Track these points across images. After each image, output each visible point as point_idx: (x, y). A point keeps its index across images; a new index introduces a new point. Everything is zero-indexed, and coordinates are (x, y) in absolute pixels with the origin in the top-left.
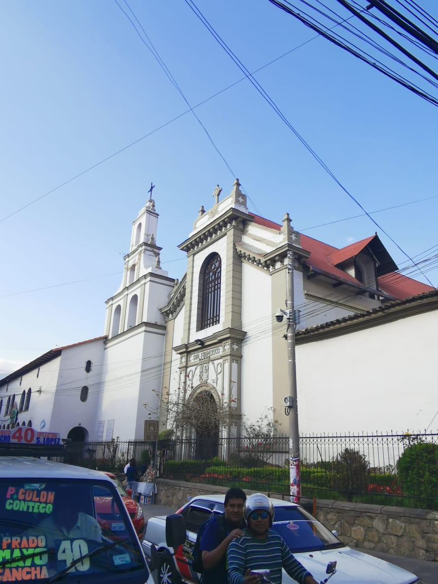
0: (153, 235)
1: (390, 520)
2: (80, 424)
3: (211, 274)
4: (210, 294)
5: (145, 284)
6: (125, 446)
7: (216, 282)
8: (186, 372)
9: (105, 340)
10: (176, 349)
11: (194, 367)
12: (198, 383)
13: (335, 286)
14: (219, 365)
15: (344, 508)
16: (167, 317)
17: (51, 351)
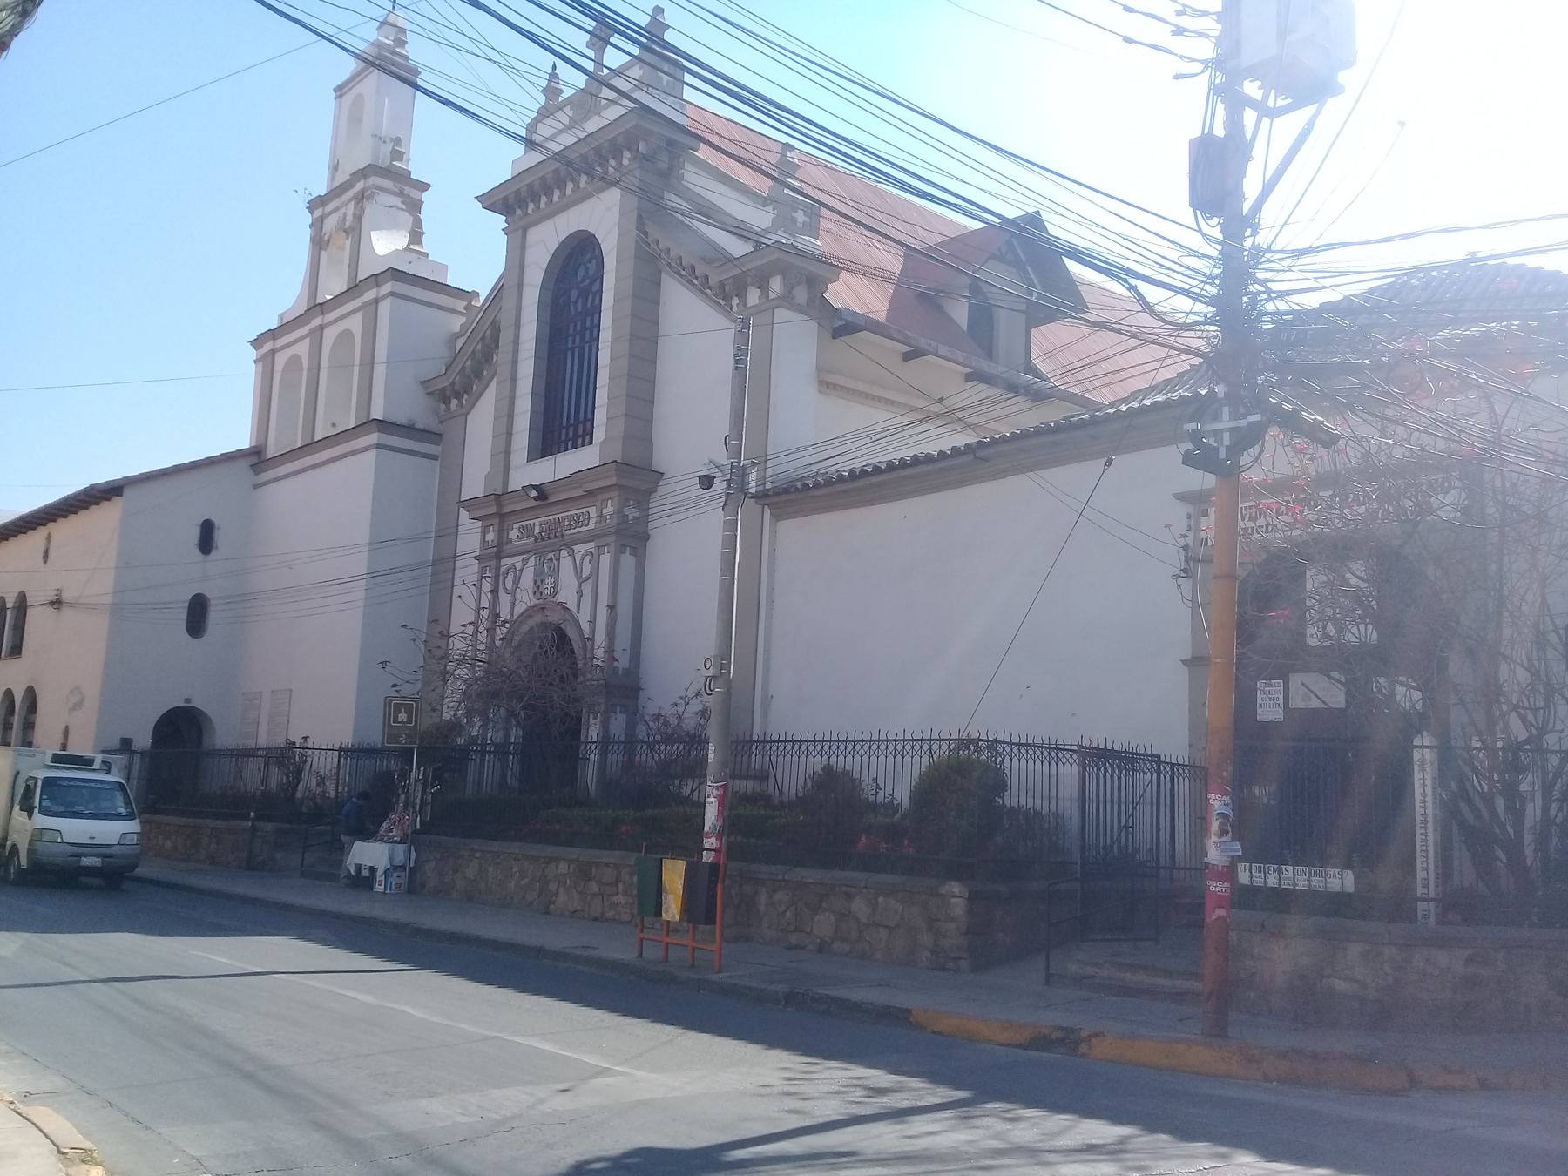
0: (398, 141)
1: (881, 899)
2: (188, 700)
3: (575, 293)
4: (569, 353)
5: (377, 301)
6: (329, 759)
7: (589, 319)
8: (498, 567)
9: (256, 458)
10: (470, 504)
11: (521, 557)
12: (534, 601)
13: (907, 357)
14: (588, 558)
15: (804, 880)
16: (443, 406)
17: (92, 487)
